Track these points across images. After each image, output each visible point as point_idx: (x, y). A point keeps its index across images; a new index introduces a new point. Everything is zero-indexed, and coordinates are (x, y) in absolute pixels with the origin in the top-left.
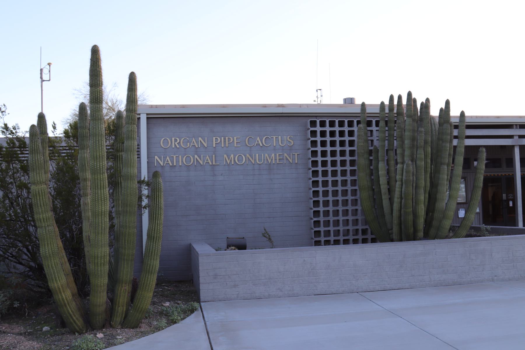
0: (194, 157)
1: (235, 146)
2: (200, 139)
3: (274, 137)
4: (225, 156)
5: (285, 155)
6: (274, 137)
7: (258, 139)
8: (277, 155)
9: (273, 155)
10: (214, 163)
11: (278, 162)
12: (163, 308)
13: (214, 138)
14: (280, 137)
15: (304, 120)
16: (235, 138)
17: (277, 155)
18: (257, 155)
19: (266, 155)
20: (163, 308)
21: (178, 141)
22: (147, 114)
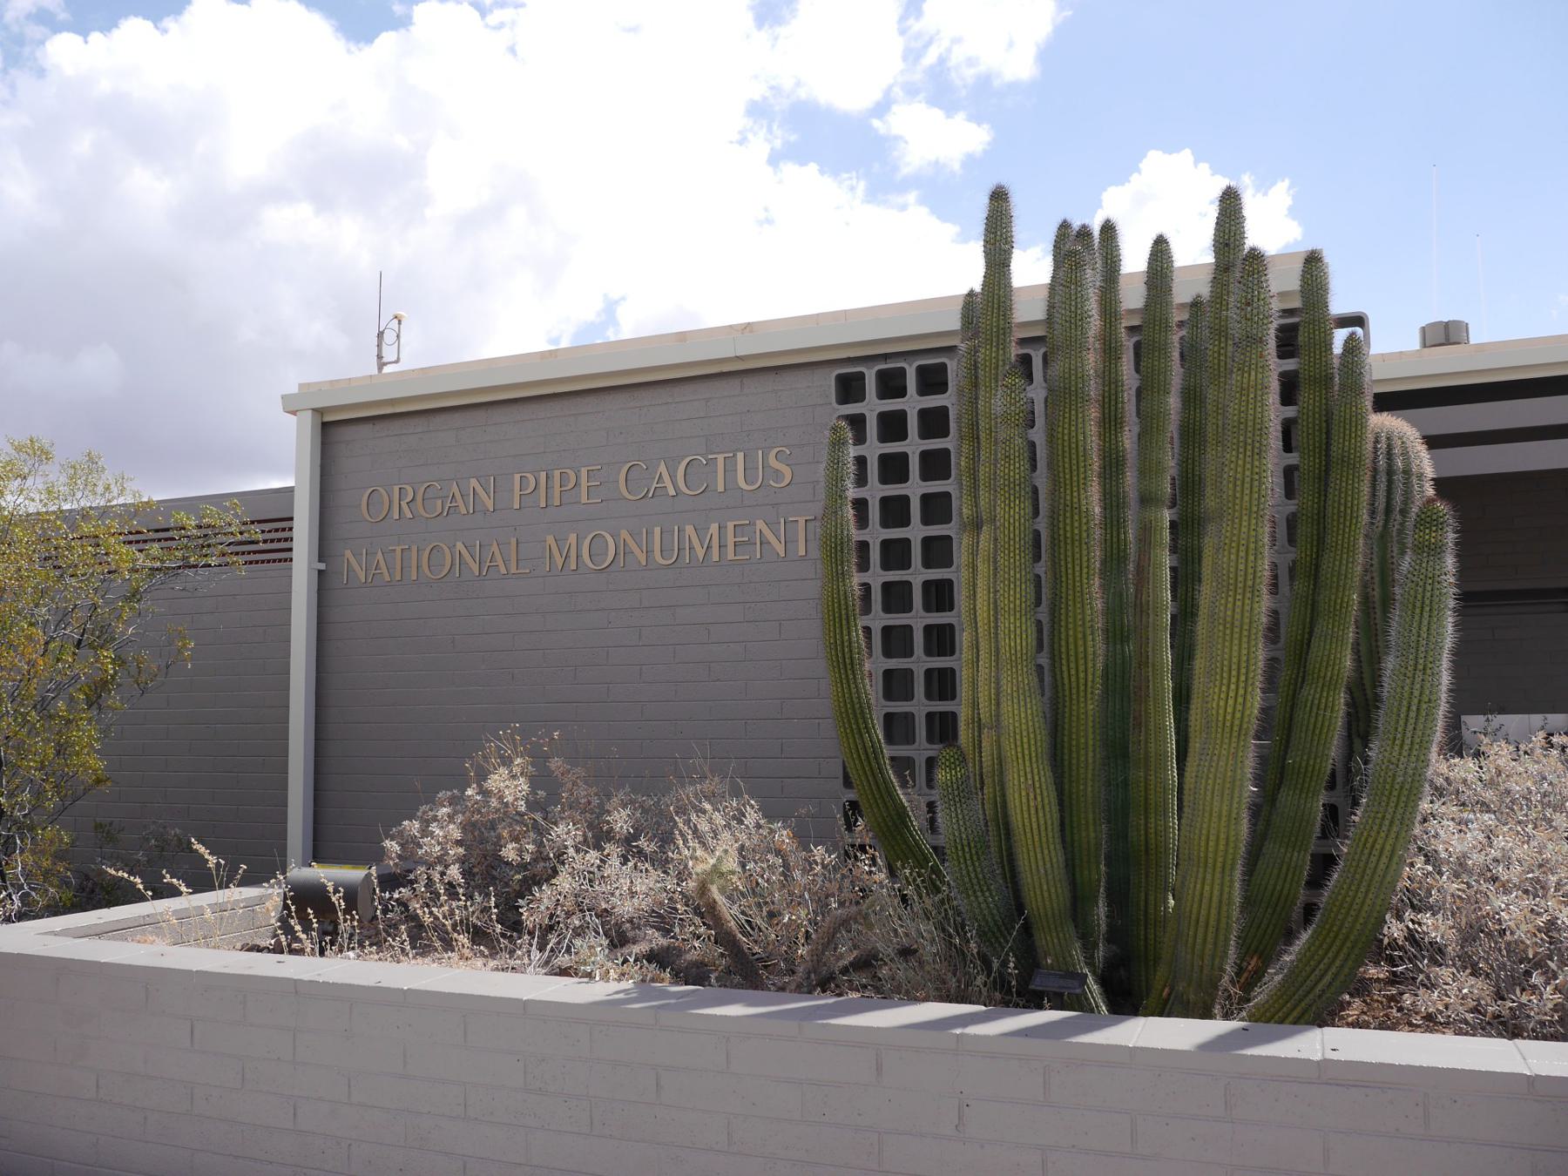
0: (452, 548)
1: (584, 499)
2: (474, 482)
3: (721, 458)
4: (550, 540)
5: (760, 524)
6: (721, 458)
7: (662, 468)
8: (730, 525)
9: (714, 528)
10: (513, 570)
11: (731, 556)
12: (633, 889)
13: (517, 477)
14: (740, 456)
15: (801, 381)
16: (584, 471)
17: (730, 525)
18: (657, 530)
19: (689, 529)
20: (633, 889)
21: (410, 498)
22: (318, 412)
